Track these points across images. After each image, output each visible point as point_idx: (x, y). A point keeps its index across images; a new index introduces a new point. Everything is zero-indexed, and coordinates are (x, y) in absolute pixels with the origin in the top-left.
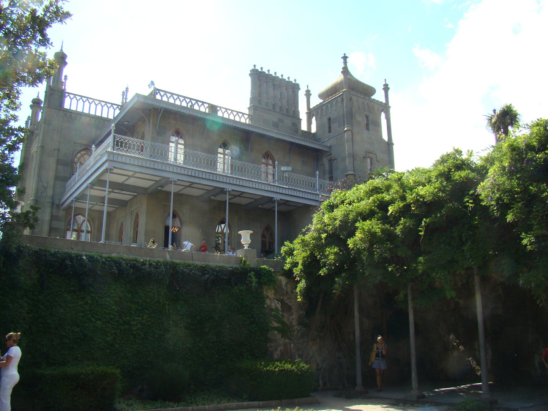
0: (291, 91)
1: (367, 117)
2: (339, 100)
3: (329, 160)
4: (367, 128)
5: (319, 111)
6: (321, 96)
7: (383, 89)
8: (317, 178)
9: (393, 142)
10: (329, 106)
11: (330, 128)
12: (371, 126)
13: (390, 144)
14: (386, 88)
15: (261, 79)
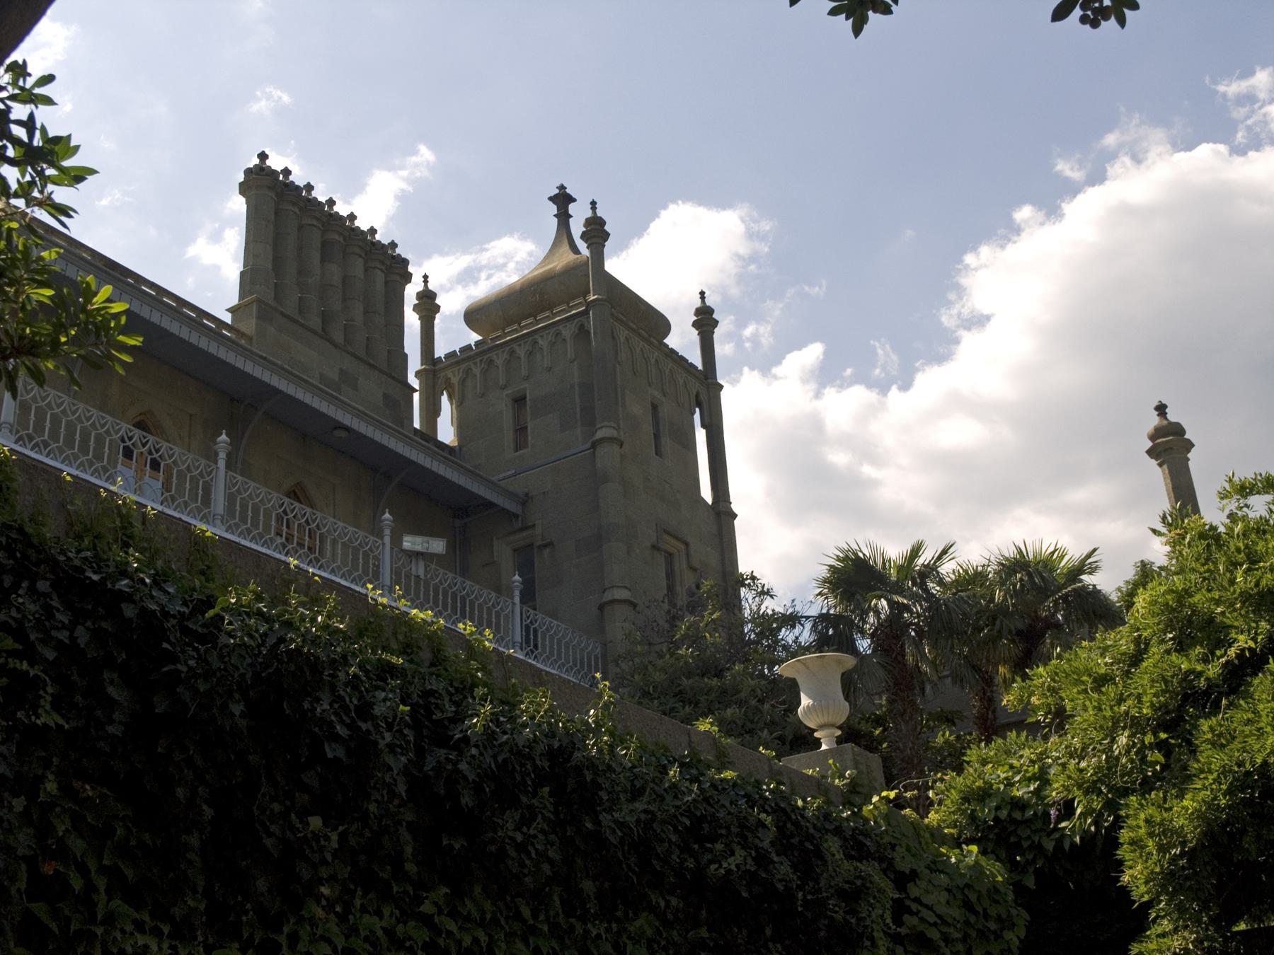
0: (380, 278)
1: (655, 407)
2: (568, 332)
3: (515, 550)
4: (658, 452)
5: (477, 371)
6: (473, 316)
7: (695, 324)
8: (517, 600)
9: (735, 507)
10: (521, 352)
11: (521, 431)
12: (667, 442)
13: (722, 513)
14: (705, 320)
15: (284, 215)
